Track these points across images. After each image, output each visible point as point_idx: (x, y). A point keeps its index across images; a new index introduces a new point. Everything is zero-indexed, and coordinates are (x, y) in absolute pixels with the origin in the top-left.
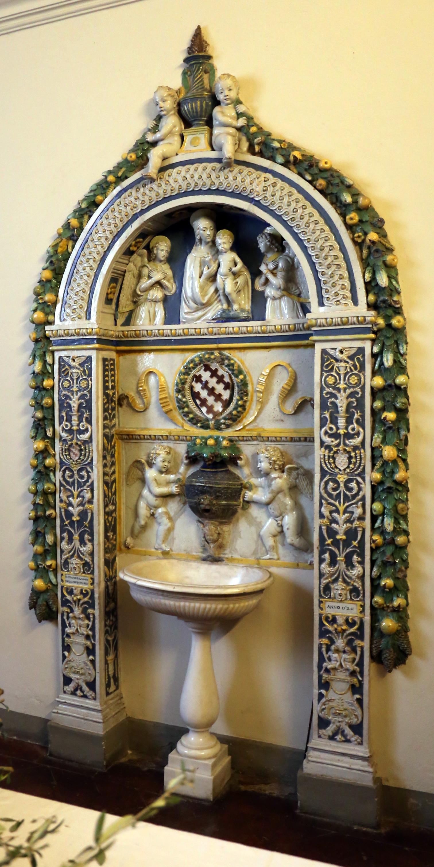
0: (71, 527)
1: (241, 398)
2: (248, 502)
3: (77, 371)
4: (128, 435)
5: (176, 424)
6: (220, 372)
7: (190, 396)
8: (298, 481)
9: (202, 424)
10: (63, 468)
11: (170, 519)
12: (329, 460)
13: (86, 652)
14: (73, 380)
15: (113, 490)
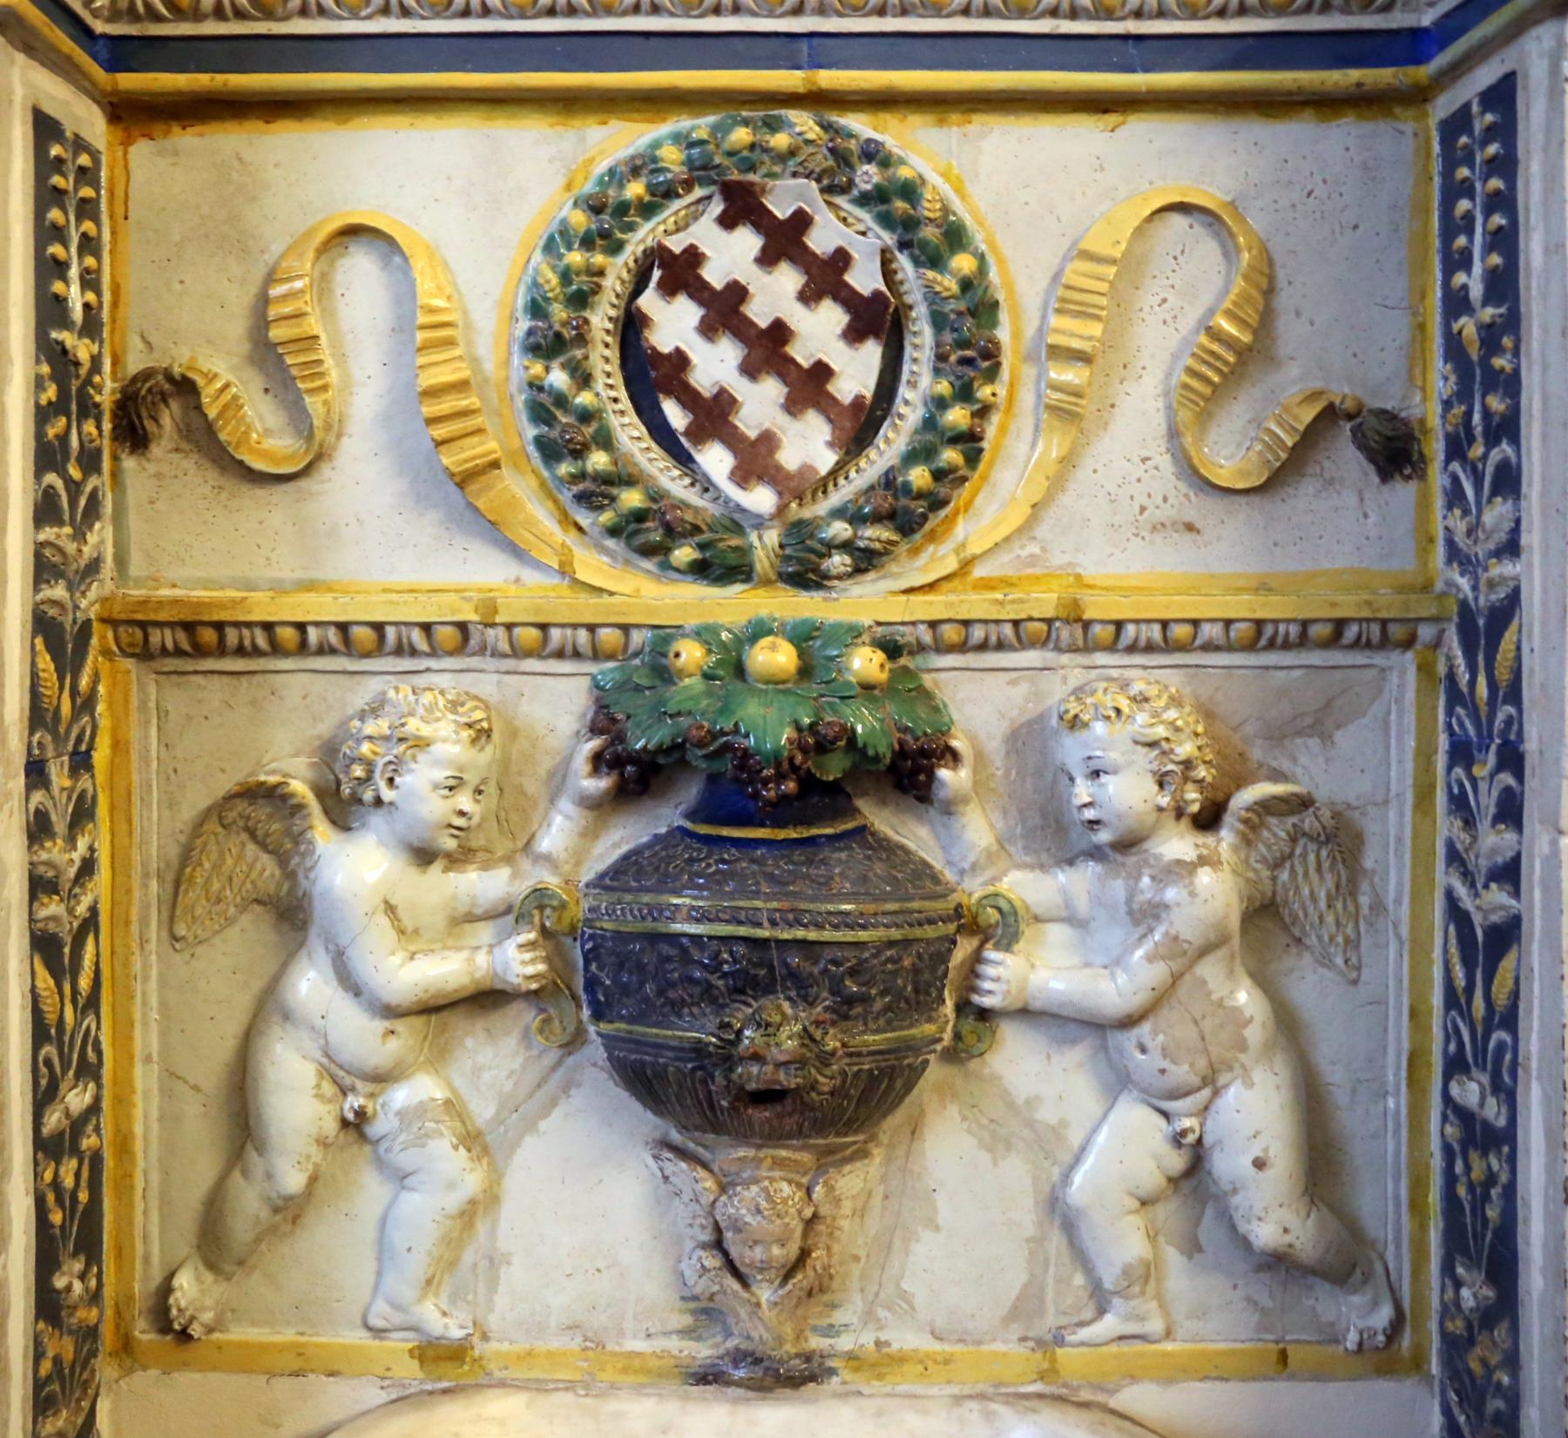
1: (964, 393)
2: (984, 1014)
4: (189, 627)
5: (516, 552)
6: (823, 238)
7: (618, 380)
8: (1284, 876)
9: (702, 547)
11: (473, 1140)
15: (84, 983)
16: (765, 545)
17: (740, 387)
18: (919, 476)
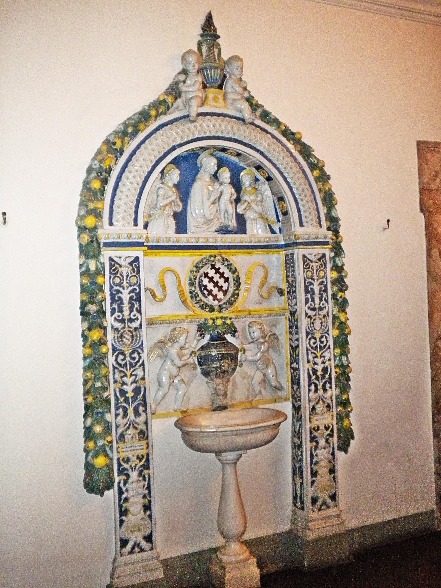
0: (125, 403)
3: (127, 268)
10: (116, 354)
12: (310, 324)
13: (143, 509)
14: (123, 277)
16: (216, 308)
17: (213, 289)
18: (233, 299)
